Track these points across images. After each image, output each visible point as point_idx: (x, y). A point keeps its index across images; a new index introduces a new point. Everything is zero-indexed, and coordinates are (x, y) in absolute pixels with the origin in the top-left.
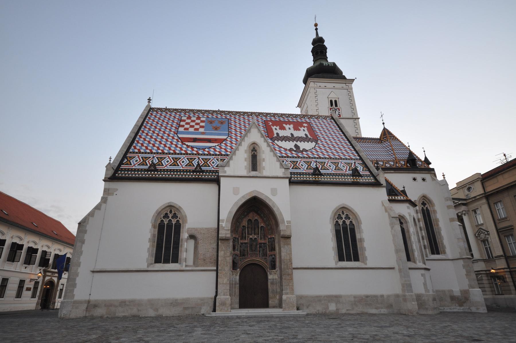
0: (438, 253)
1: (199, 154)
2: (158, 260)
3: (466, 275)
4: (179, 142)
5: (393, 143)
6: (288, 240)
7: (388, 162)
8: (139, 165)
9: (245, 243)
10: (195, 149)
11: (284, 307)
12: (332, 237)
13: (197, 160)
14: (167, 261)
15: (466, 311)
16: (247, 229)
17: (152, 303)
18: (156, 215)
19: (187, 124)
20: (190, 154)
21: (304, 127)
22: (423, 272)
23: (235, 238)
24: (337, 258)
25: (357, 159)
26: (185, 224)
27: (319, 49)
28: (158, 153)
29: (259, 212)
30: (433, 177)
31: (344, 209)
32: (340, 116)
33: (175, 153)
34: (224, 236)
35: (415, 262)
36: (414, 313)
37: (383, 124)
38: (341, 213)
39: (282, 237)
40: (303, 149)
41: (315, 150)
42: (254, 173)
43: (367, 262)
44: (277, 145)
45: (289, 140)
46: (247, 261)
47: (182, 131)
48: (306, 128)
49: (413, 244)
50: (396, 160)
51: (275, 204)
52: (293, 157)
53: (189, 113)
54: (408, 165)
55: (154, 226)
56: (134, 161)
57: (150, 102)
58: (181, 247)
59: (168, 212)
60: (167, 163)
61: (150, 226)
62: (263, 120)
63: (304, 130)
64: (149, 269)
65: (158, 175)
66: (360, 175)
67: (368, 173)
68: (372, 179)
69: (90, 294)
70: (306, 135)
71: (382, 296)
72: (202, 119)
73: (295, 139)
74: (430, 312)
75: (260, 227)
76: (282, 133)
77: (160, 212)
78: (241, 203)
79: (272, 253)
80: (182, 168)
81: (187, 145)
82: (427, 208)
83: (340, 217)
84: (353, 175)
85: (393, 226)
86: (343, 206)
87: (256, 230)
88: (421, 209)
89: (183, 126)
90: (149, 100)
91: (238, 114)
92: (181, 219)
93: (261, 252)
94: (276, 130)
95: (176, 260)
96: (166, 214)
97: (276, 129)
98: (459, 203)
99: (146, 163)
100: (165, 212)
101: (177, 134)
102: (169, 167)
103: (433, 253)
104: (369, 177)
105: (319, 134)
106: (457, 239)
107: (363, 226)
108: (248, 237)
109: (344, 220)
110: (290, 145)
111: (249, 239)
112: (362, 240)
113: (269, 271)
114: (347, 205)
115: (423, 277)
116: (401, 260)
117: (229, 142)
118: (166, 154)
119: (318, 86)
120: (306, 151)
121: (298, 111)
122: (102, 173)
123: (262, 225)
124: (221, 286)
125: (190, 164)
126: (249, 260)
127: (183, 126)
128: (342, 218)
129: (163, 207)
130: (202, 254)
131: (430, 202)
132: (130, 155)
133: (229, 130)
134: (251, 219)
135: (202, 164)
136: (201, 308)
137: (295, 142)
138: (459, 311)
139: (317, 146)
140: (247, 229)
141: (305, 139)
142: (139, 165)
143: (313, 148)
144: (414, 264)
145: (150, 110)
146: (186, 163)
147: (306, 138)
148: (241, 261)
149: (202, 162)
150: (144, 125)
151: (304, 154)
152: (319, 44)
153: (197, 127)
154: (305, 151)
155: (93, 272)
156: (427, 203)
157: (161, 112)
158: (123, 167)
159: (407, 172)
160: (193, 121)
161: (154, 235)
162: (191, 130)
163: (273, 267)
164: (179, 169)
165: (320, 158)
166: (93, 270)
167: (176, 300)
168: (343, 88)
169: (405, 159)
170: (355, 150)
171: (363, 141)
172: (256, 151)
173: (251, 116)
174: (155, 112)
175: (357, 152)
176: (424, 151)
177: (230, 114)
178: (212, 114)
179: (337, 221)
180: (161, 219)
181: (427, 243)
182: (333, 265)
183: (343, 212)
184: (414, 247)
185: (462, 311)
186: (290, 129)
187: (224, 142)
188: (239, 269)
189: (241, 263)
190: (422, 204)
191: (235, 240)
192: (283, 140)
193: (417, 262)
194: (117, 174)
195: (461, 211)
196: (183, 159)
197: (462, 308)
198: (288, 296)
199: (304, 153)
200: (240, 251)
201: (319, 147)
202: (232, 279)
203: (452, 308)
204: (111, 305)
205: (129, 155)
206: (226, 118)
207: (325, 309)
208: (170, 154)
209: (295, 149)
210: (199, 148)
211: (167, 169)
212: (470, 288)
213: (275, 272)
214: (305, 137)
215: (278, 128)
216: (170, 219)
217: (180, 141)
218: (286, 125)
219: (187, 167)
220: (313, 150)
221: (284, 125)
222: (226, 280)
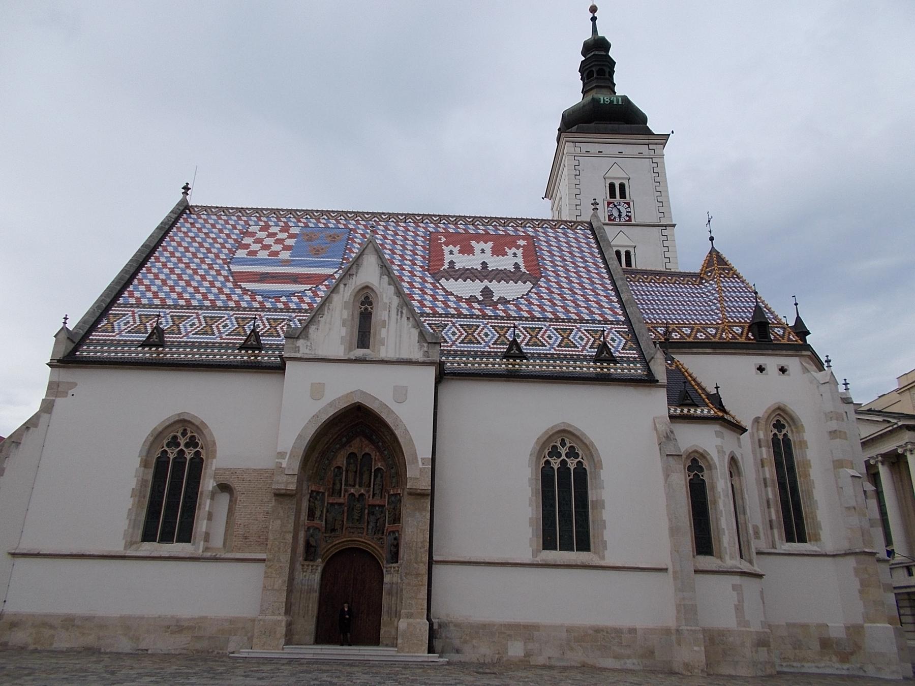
0: (802, 539)
1: (263, 308)
2: (148, 536)
3: (861, 592)
4: (229, 281)
5: (727, 283)
6: (422, 501)
7: (703, 328)
8: (129, 332)
9: (340, 504)
10: (259, 298)
11: (399, 646)
12: (530, 495)
14: (167, 538)
15: (856, 673)
16: (344, 473)
17: (127, 625)
18: (151, 439)
20: (244, 309)
21: (518, 247)
22: (737, 580)
23: (318, 493)
25: (618, 322)
26: (210, 461)
27: (595, 65)
29: (374, 437)
30: (805, 364)
31: (565, 435)
32: (630, 220)
33: (214, 307)
35: (721, 558)
36: (696, 671)
37: (712, 239)
38: (558, 444)
39: (410, 494)
40: (500, 298)
42: (360, 352)
43: (606, 553)
44: (444, 289)
46: (339, 543)
49: (722, 516)
50: (723, 323)
51: (401, 421)
52: (471, 316)
54: (750, 335)
55: (145, 464)
56: (122, 324)
57: (188, 194)
58: (199, 509)
59: (179, 435)
60: (189, 329)
61: (136, 462)
63: (515, 255)
64: (130, 553)
65: (169, 354)
66: (612, 359)
67: (634, 354)
69: (5, 601)
70: (517, 266)
71: (633, 631)
74: (743, 672)
75: (373, 471)
76: (463, 262)
77: (161, 433)
78: (325, 418)
79: (393, 527)
80: (218, 340)
81: (244, 290)
82: (785, 435)
83: (554, 452)
84: (597, 359)
85: (668, 476)
86: (562, 428)
87: (366, 477)
90: (186, 188)
91: (376, 219)
92: (204, 448)
93: (371, 523)
94: (453, 256)
95: (186, 536)
96: (175, 437)
98: (900, 424)
100: (172, 434)
101: (228, 264)
103: (790, 539)
104: (632, 362)
106: (847, 508)
107: (604, 474)
108: (346, 491)
109: (564, 459)
110: (472, 288)
111: (346, 496)
112: (600, 504)
113: (384, 564)
114: (570, 425)
115: (735, 593)
116: (678, 552)
118: (195, 308)
119: (583, 150)
120: (508, 302)
121: (543, 210)
122: (46, 349)
123: (379, 465)
124: (268, 593)
126: (345, 539)
127: (247, 246)
129: (167, 424)
130: (242, 526)
131: (793, 420)
133: (345, 253)
134: (356, 451)
137: (486, 283)
138: (839, 672)
140: (344, 473)
141: (508, 273)
142: (129, 332)
143: (523, 295)
144: (719, 562)
145: (183, 210)
146: (230, 328)
147: (514, 273)
148: (326, 541)
151: (498, 309)
152: (597, 53)
153: (278, 247)
155: (14, 555)
156: (786, 425)
157: (208, 215)
159: (744, 351)
160: (272, 235)
161: (143, 483)
162: (263, 255)
163: (395, 557)
165: (533, 318)
166: (13, 551)
167: (178, 621)
168: (640, 156)
169: (746, 322)
170: (620, 301)
171: (658, 279)
172: (371, 304)
173: (405, 222)
175: (623, 307)
176: (796, 304)
178: (318, 220)
179: (547, 462)
180: (163, 447)
181: (778, 517)
182: (527, 558)
183: (563, 440)
184: (723, 523)
185: (844, 672)
186: (483, 251)
187: (326, 283)
188: (320, 560)
189: (325, 547)
190: (774, 426)
191: (314, 496)
193: (727, 558)
195: (902, 443)
196: (227, 319)
197: (846, 666)
198: (411, 620)
200: (326, 519)
202: (302, 580)
203: (823, 665)
204: (44, 624)
205: (114, 310)
206: (346, 227)
207: (499, 653)
208: (201, 307)
209: (480, 298)
210: (266, 295)
211: (186, 342)
212: (865, 622)
213: (397, 568)
214: (513, 270)
215: (456, 250)
216: (180, 448)
217: (232, 280)
220: (522, 301)
221: (473, 243)
222: (280, 581)
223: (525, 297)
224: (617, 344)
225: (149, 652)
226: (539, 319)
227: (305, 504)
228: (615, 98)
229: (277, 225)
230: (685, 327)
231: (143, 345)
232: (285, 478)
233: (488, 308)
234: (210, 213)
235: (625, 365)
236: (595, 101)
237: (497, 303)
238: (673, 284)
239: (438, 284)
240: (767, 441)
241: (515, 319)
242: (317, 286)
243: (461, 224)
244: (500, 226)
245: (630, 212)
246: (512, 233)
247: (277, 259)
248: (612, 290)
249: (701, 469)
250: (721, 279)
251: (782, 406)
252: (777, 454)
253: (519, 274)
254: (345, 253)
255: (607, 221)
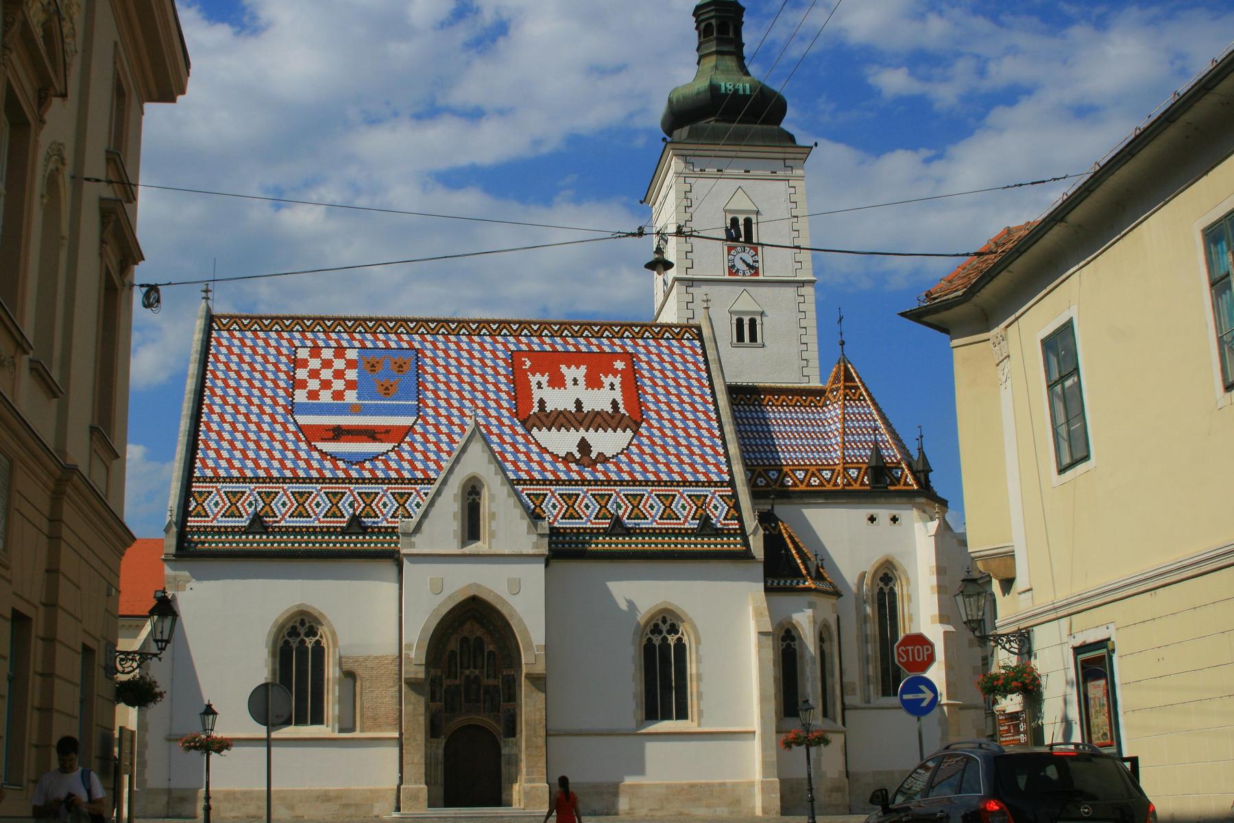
1: (349, 480)
10: (341, 464)
13: (347, 500)
18: (275, 630)
19: (314, 374)
21: (615, 373)
24: (641, 713)
25: (722, 483)
28: (257, 479)
32: (757, 274)
33: (296, 479)
34: (413, 676)
37: (842, 343)
38: (660, 622)
41: (628, 456)
45: (568, 425)
47: (303, 404)
48: (619, 375)
52: (571, 482)
53: (312, 331)
59: (298, 625)
62: (507, 349)
63: (612, 386)
68: (739, 544)
70: (614, 404)
72: (352, 354)
73: (583, 420)
75: (486, 654)
78: (445, 611)
80: (316, 524)
81: (321, 452)
88: (876, 591)
89: (302, 384)
96: (294, 628)
97: (539, 385)
99: (238, 509)
101: (292, 413)
102: (290, 522)
105: (650, 398)
108: (462, 673)
111: (463, 677)
117: (418, 438)
118: (278, 480)
123: (491, 647)
125: (333, 513)
127: (302, 384)
128: (660, 632)
132: (199, 487)
135: (360, 510)
136: (372, 806)
139: (635, 442)
141: (607, 417)
143: (623, 449)
146: (324, 507)
147: (613, 417)
149: (360, 505)
150: (208, 384)
153: (339, 385)
154: (600, 463)
158: (192, 524)
160: (327, 364)
164: (311, 525)
165: (634, 482)
169: (864, 462)
172: (478, 494)
173: (479, 335)
174: (225, 334)
177: (422, 329)
179: (650, 640)
186: (575, 381)
187: (408, 439)
188: (443, 737)
190: (882, 579)
192: (553, 424)
194: (185, 542)
199: (599, 467)
201: (639, 446)
206: (412, 348)
208: (284, 480)
209: (578, 456)
214: (610, 411)
215: (544, 379)
217: (304, 439)
218: (569, 367)
219: (329, 519)
220: (622, 457)
221: (563, 368)
222: (418, 756)
223: (625, 451)
224: (719, 513)
225: (305, 817)
226: (640, 483)
227: (428, 688)
228: (741, 85)
229: (329, 347)
230: (800, 470)
231: (246, 531)
232: (413, 668)
233: (586, 469)
234: (243, 328)
235: (725, 539)
236: (714, 88)
237: (594, 463)
238: (793, 407)
239: (530, 437)
240: (872, 595)
241: (615, 483)
242: (399, 445)
243: (546, 336)
244: (593, 337)
245: (757, 262)
246: (607, 350)
247: (344, 404)
248: (718, 438)
249: (793, 639)
250: (846, 402)
251: (890, 559)
252: (881, 606)
253: (618, 417)
254: (418, 392)
255: (727, 277)
